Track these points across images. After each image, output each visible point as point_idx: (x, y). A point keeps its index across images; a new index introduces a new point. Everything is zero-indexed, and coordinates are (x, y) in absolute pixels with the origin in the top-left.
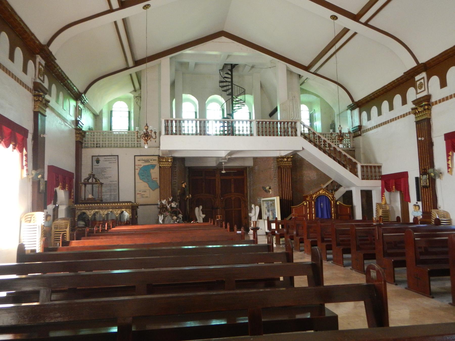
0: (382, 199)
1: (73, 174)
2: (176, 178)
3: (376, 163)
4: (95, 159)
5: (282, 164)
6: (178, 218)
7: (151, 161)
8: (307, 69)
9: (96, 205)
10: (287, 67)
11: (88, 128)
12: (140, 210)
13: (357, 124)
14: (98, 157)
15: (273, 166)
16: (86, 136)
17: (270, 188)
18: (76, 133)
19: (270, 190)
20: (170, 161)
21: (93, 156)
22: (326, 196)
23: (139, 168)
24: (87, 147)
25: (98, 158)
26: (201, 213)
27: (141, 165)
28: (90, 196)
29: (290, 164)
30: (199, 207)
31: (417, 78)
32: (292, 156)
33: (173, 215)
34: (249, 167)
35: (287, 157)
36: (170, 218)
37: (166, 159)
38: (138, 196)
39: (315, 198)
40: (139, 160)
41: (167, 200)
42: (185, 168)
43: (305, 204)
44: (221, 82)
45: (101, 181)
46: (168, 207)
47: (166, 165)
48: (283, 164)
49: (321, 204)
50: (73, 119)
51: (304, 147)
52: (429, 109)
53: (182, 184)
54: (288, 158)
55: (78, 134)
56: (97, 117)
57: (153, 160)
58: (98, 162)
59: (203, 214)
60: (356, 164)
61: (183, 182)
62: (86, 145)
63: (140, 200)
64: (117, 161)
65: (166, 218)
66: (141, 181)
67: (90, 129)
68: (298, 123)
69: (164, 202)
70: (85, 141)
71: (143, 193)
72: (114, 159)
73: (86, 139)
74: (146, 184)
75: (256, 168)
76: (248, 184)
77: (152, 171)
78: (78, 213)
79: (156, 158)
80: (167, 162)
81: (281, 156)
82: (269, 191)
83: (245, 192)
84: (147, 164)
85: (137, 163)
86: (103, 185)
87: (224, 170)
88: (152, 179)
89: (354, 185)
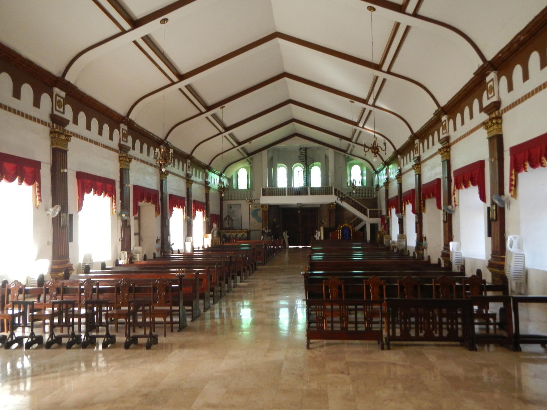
4: (229, 206)
6: (271, 237)
17: (325, 221)
21: (228, 205)
24: (225, 200)
28: (228, 226)
37: (265, 206)
38: (251, 226)
44: (299, 157)
45: (233, 218)
46: (266, 232)
53: (274, 220)
54: (333, 205)
58: (231, 208)
63: (252, 228)
65: (265, 238)
69: (264, 229)
77: (259, 212)
78: (222, 234)
84: (255, 209)
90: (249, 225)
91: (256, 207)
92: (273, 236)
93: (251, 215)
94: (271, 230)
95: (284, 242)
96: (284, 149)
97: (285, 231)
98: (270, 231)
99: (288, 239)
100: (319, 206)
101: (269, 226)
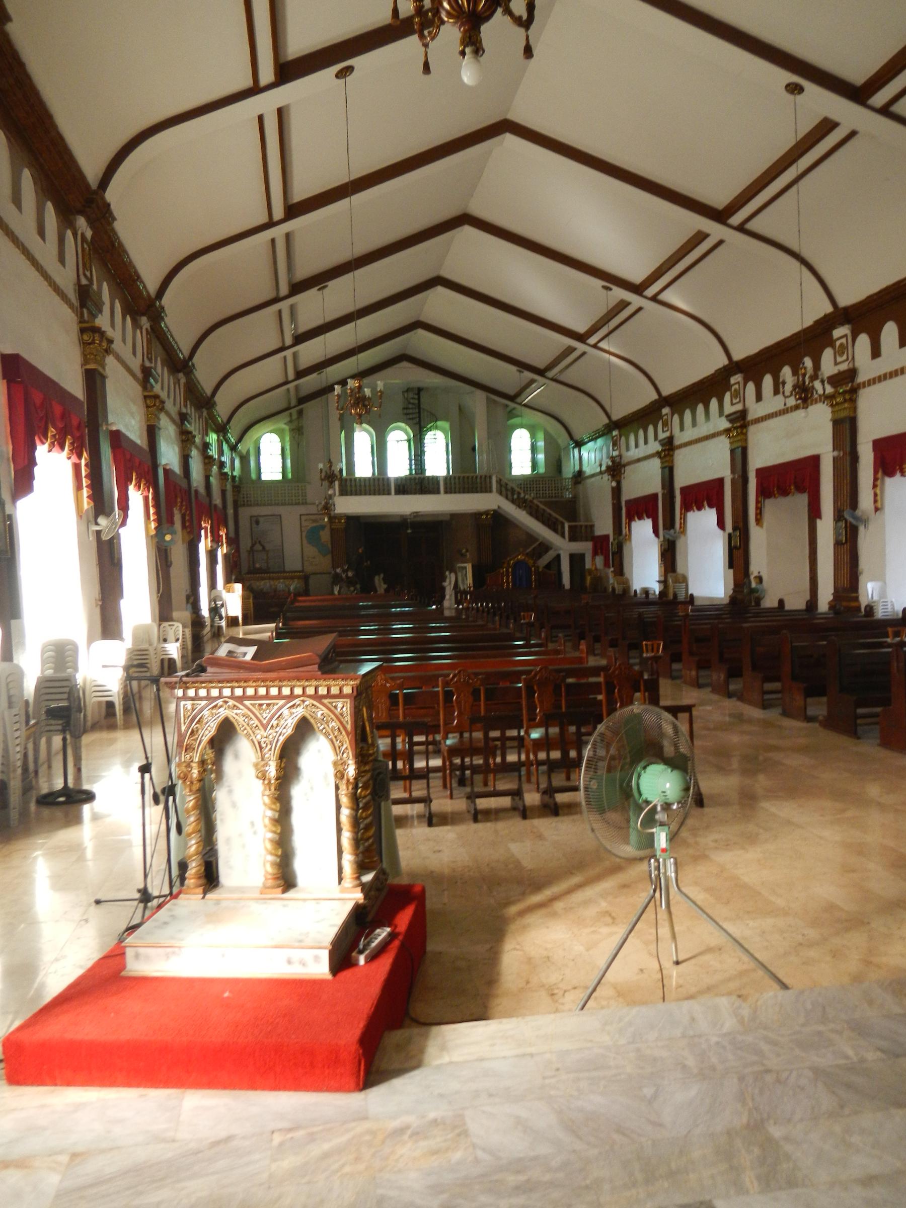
4: (254, 519)
12: (312, 581)
13: (577, 468)
17: (467, 551)
20: (343, 521)
21: (251, 517)
26: (382, 584)
40: (305, 520)
41: (342, 568)
43: (502, 571)
46: (344, 576)
58: (257, 523)
59: (385, 583)
60: (563, 524)
63: (309, 569)
65: (343, 590)
69: (339, 570)
77: (322, 533)
84: (315, 525)
85: (304, 524)
89: (560, 549)
91: (314, 521)
93: (305, 541)
97: (379, 575)
100: (447, 518)
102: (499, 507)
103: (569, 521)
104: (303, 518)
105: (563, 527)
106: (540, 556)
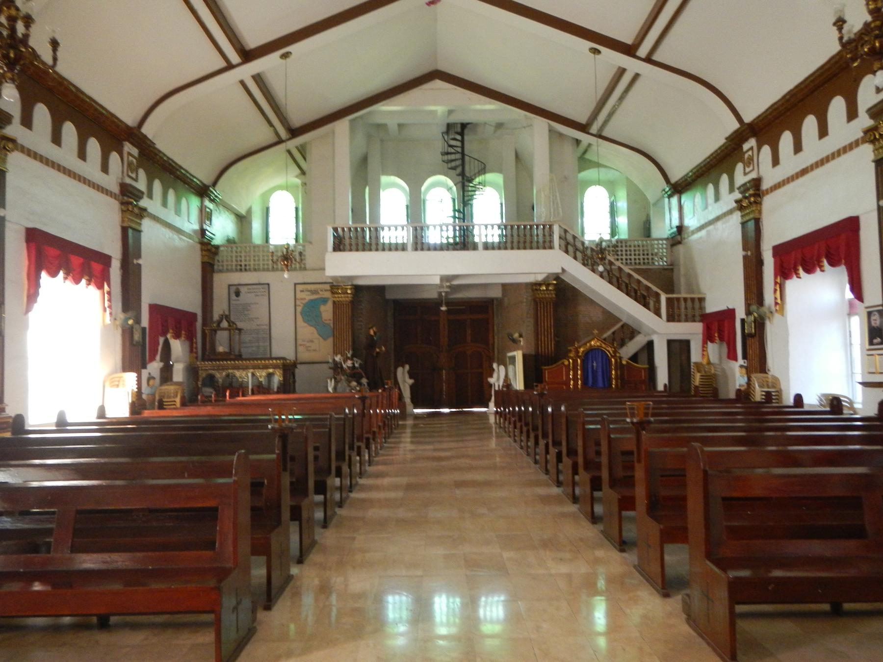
0: (703, 355)
1: (194, 315)
2: (361, 319)
3: (700, 293)
4: (233, 289)
5: (539, 294)
7: (320, 292)
8: (583, 128)
9: (229, 362)
10: (550, 126)
11: (226, 239)
12: (300, 371)
13: (676, 222)
14: (239, 287)
15: (526, 297)
16: (221, 254)
17: (521, 336)
18: (202, 250)
19: (521, 339)
21: (230, 286)
22: (602, 350)
23: (302, 303)
24: (221, 271)
25: (238, 289)
27: (305, 299)
29: (552, 294)
30: (403, 367)
31: (746, 146)
32: (555, 282)
33: (350, 379)
34: (497, 299)
35: (546, 282)
36: (346, 385)
37: (342, 289)
38: (300, 349)
39: (582, 354)
40: (302, 291)
42: (387, 301)
45: (240, 325)
46: (344, 366)
47: (344, 299)
48: (540, 295)
49: (593, 362)
50: (196, 227)
51: (565, 268)
52: (758, 203)
53: (370, 329)
54: (548, 285)
55: (205, 251)
56: (243, 220)
57: (326, 290)
58: (238, 294)
60: (658, 296)
61: (370, 326)
62: (221, 268)
63: (304, 356)
64: (267, 292)
65: (339, 385)
66: (305, 325)
67: (230, 241)
68: (555, 227)
69: (338, 358)
70: (218, 261)
71: (309, 344)
72: (263, 290)
73: (220, 259)
74: (312, 329)
75: (506, 299)
76: (495, 328)
77: (323, 308)
78: (203, 374)
79: (328, 287)
80: (344, 294)
81: (537, 281)
82: (520, 341)
83: (491, 342)
86: (242, 331)
87: (444, 305)
88: (323, 320)
89: (655, 332)
90: (293, 348)
91: (314, 292)
92: (367, 378)
93: (299, 318)
94: (359, 361)
95: (401, 397)
96: (400, 126)
98: (357, 365)
99: (412, 387)
100: (497, 293)
101: (353, 350)
102: (563, 270)
103: (666, 292)
104: (299, 288)
105: (658, 301)
106: (622, 344)
